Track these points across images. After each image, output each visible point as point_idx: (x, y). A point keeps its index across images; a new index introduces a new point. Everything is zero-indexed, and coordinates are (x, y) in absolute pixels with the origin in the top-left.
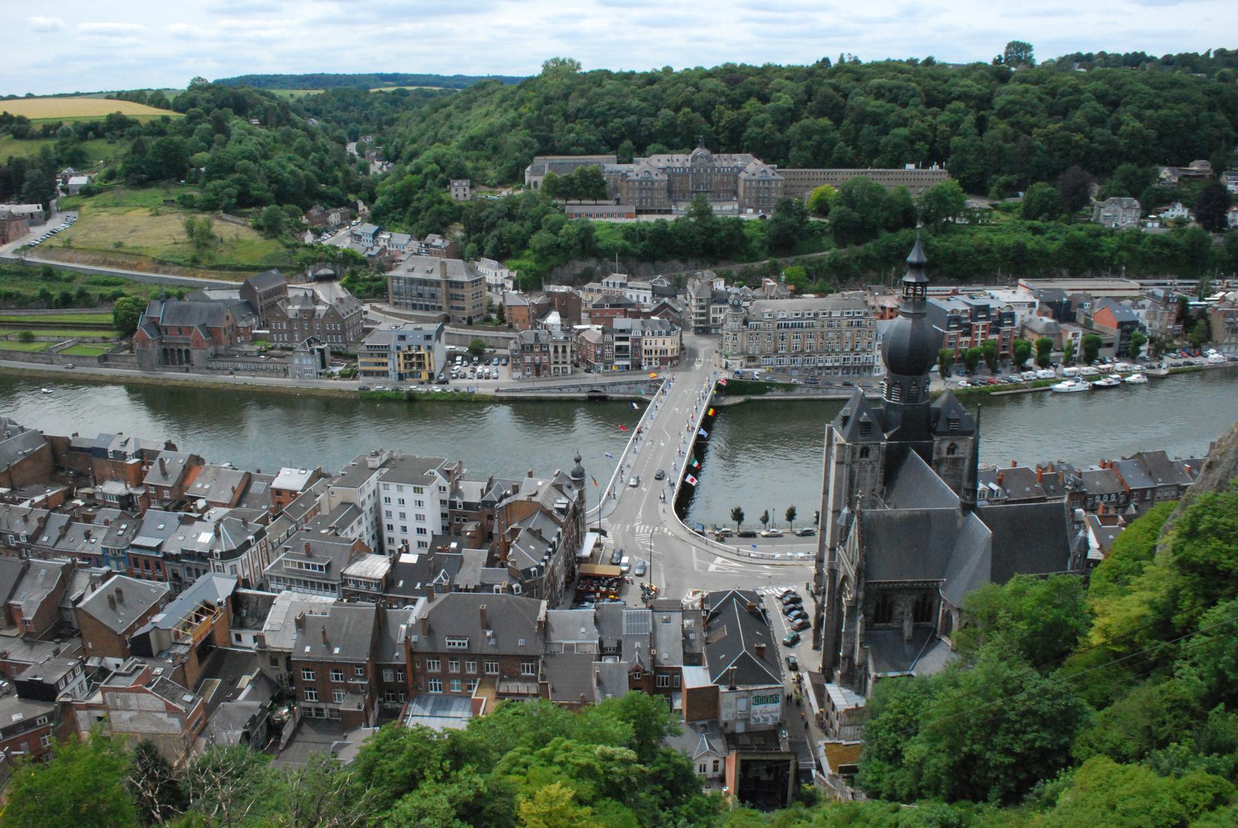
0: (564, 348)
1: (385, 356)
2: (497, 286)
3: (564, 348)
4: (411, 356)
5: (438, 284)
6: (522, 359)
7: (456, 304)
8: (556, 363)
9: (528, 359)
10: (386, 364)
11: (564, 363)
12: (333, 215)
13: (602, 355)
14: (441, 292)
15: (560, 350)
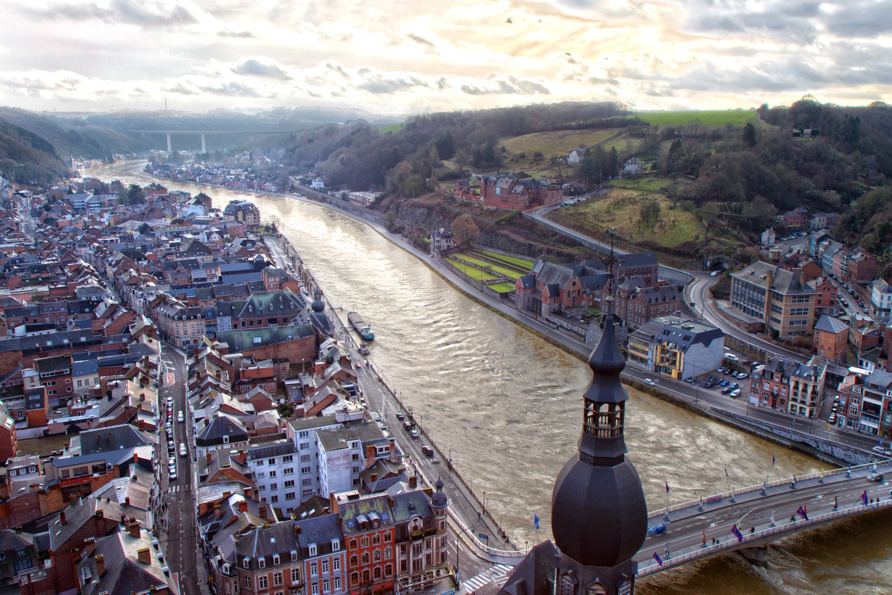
0: (806, 386)
1: (646, 345)
2: (881, 310)
3: (806, 386)
4: (668, 351)
5: (762, 292)
6: (761, 385)
7: (775, 315)
8: (795, 400)
9: (767, 387)
10: (646, 353)
11: (803, 402)
12: (817, 219)
13: (847, 406)
14: (765, 298)
15: (801, 387)
